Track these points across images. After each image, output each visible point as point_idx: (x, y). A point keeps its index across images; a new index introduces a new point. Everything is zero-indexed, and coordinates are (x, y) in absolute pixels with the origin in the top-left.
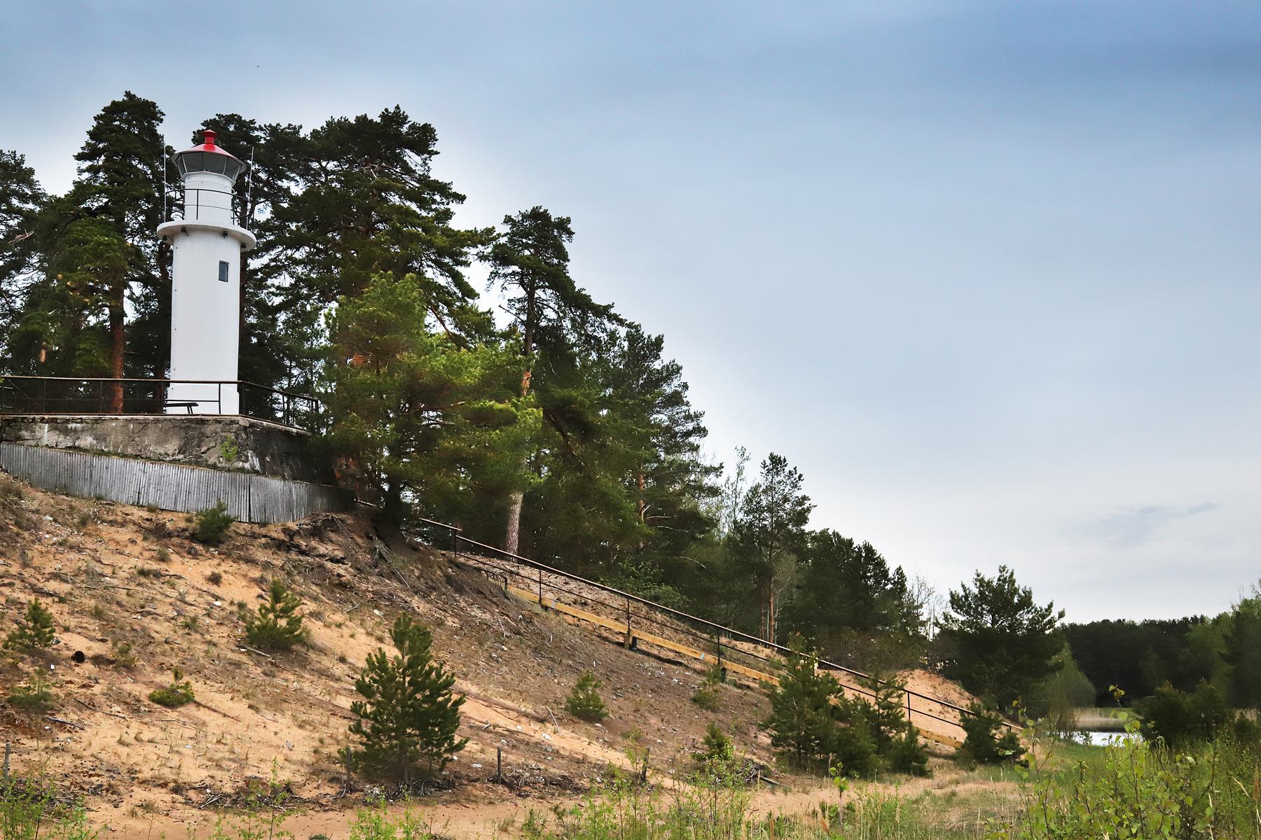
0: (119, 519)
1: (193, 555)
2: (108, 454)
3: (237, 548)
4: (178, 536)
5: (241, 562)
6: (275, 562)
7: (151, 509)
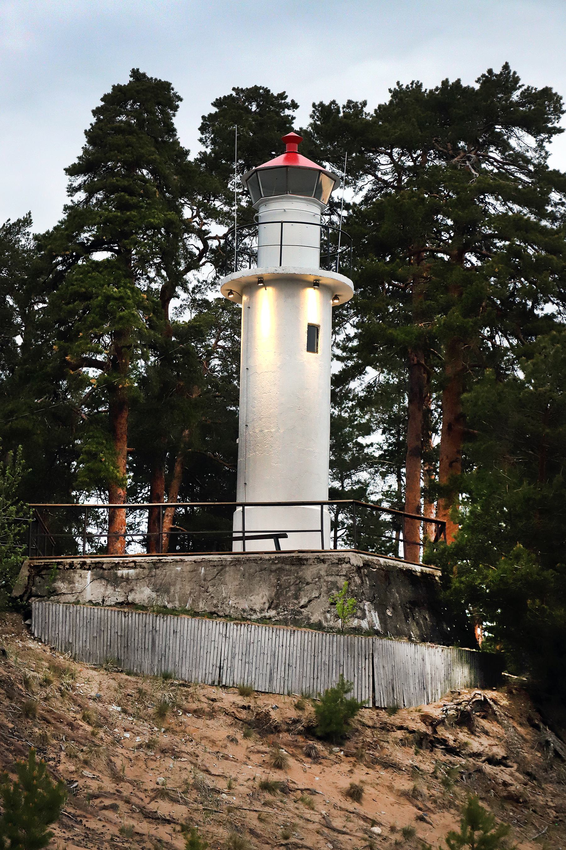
0: (205, 706)
1: (314, 758)
2: (174, 612)
3: (369, 746)
4: (288, 731)
5: (378, 767)
6: (423, 767)
7: (244, 692)
